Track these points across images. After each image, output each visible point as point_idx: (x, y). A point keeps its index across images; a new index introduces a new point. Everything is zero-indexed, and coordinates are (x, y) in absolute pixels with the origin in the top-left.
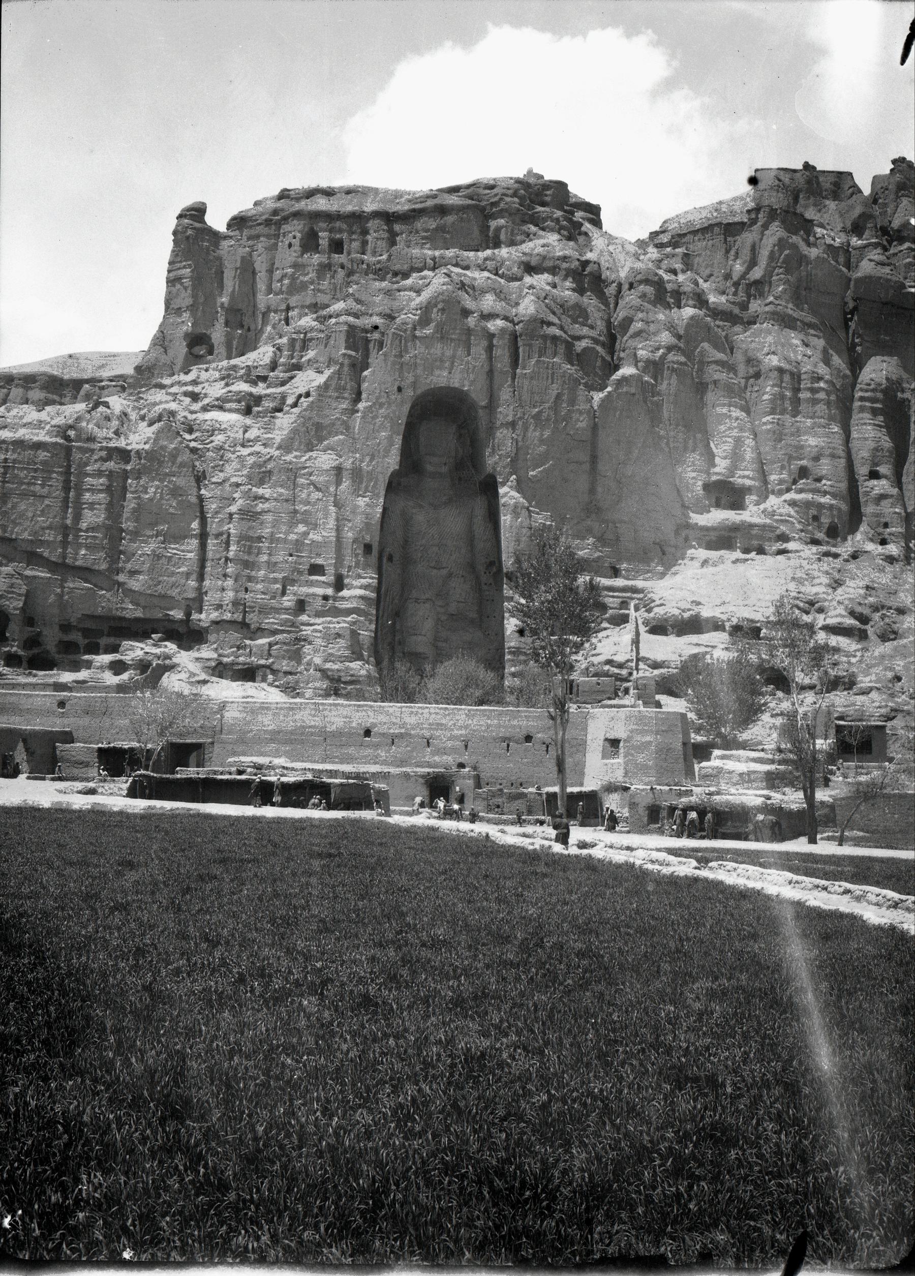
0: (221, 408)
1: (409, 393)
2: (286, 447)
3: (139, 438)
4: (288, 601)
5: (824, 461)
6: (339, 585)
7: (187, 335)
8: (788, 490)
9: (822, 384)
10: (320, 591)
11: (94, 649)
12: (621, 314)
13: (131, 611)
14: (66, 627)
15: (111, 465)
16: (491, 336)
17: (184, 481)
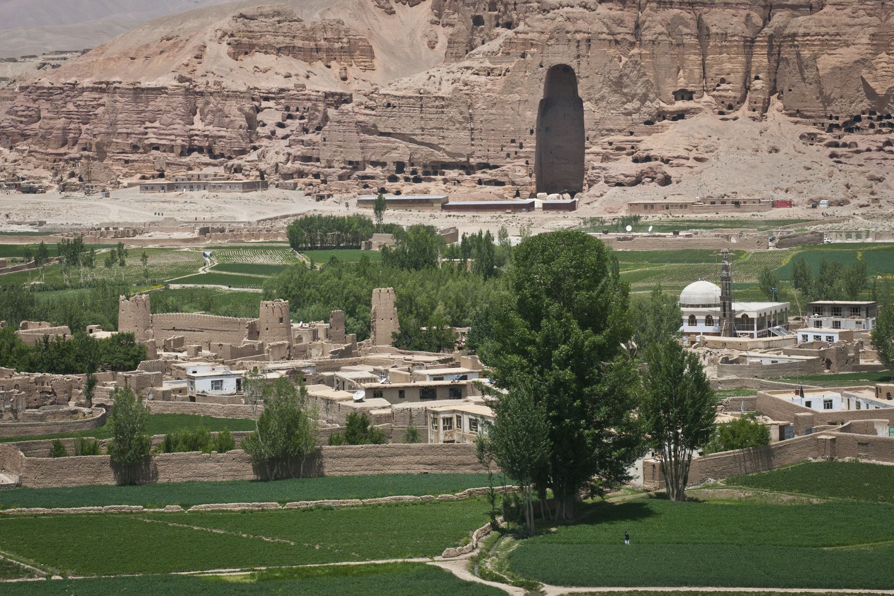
0: (478, 74)
1: (546, 67)
2: (501, 93)
3: (446, 90)
4: (503, 154)
5: (732, 75)
6: (521, 147)
7: (472, 17)
8: (714, 90)
9: (736, 38)
10: (514, 149)
11: (435, 174)
12: (643, 18)
13: (447, 159)
14: (425, 166)
15: (437, 103)
16: (578, 42)
17: (464, 109)
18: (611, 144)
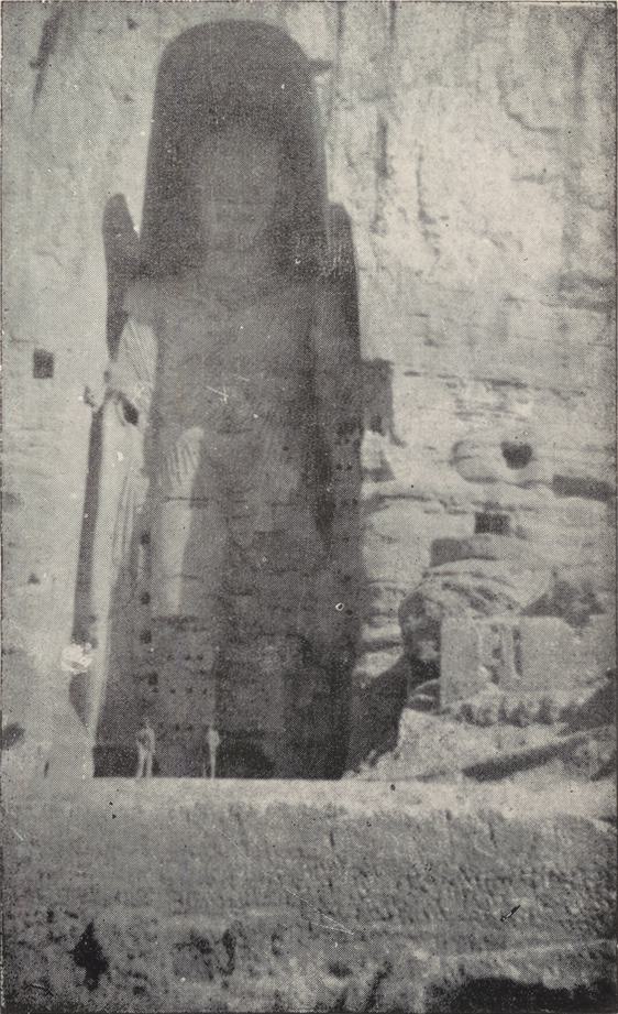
18: (518, 456)
